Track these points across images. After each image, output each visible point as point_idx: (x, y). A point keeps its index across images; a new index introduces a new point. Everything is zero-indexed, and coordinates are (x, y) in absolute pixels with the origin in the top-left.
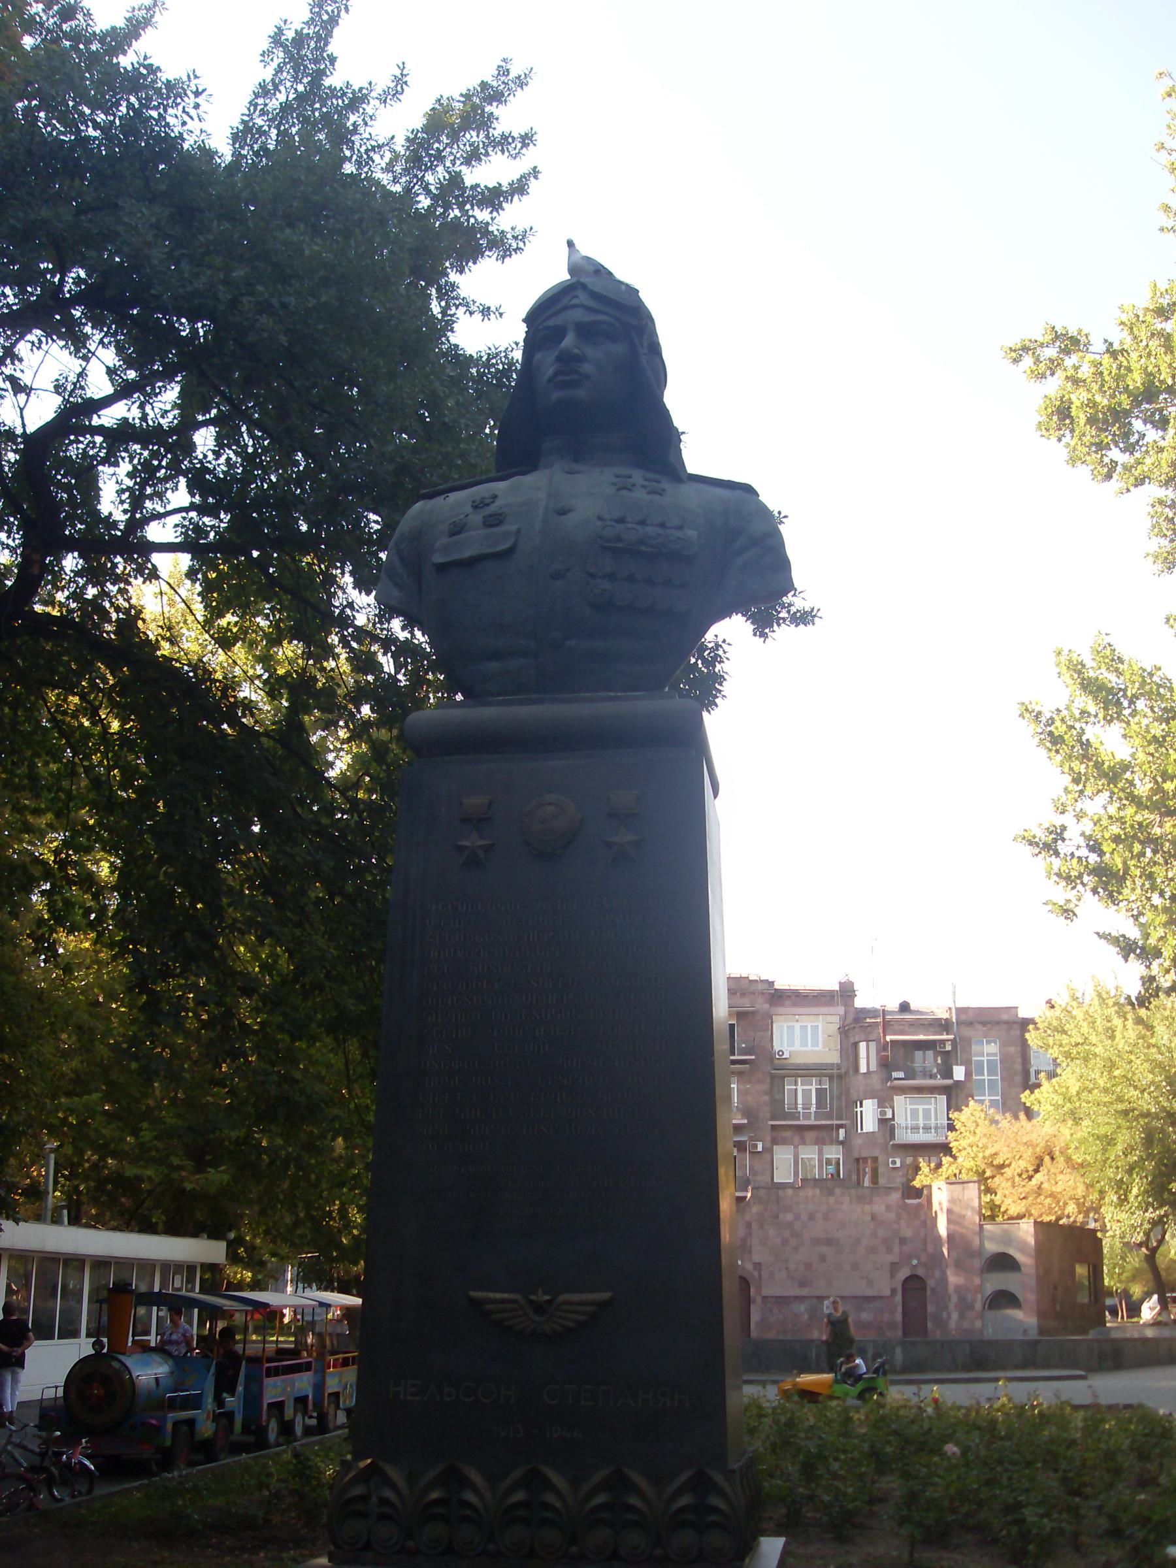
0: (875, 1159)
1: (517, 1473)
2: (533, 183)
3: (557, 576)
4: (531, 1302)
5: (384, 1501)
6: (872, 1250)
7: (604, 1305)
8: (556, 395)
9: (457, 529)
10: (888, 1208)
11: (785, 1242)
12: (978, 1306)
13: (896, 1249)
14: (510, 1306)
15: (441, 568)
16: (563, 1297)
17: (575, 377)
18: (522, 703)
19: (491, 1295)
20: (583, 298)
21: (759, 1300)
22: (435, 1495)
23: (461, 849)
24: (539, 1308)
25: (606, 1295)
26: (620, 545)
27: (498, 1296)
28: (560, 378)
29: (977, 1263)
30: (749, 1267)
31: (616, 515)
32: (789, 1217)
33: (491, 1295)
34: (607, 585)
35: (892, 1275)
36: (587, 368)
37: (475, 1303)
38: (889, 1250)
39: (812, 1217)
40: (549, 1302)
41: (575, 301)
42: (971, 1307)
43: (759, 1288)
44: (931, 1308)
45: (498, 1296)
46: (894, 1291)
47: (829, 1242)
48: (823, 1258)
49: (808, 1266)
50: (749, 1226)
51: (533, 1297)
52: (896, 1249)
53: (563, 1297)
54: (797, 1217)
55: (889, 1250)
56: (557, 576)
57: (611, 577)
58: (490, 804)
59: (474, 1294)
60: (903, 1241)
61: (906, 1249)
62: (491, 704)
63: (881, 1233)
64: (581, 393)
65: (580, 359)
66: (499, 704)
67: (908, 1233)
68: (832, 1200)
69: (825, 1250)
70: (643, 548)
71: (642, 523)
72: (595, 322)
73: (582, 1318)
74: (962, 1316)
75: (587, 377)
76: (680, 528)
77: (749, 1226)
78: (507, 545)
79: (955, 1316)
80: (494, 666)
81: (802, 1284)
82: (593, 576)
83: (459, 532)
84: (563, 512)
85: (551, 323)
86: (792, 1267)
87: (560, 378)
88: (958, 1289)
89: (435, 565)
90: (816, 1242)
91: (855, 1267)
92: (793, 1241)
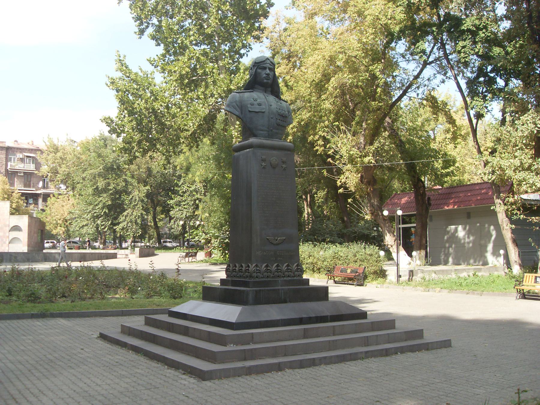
1: (276, 264)
3: (272, 118)
5: (257, 270)
7: (284, 239)
8: (265, 81)
9: (252, 105)
15: (250, 111)
18: (266, 139)
20: (268, 62)
22: (265, 269)
23: (262, 165)
57: (280, 120)
64: (270, 81)
66: (263, 139)
80: (262, 132)
84: (271, 106)
85: (264, 66)
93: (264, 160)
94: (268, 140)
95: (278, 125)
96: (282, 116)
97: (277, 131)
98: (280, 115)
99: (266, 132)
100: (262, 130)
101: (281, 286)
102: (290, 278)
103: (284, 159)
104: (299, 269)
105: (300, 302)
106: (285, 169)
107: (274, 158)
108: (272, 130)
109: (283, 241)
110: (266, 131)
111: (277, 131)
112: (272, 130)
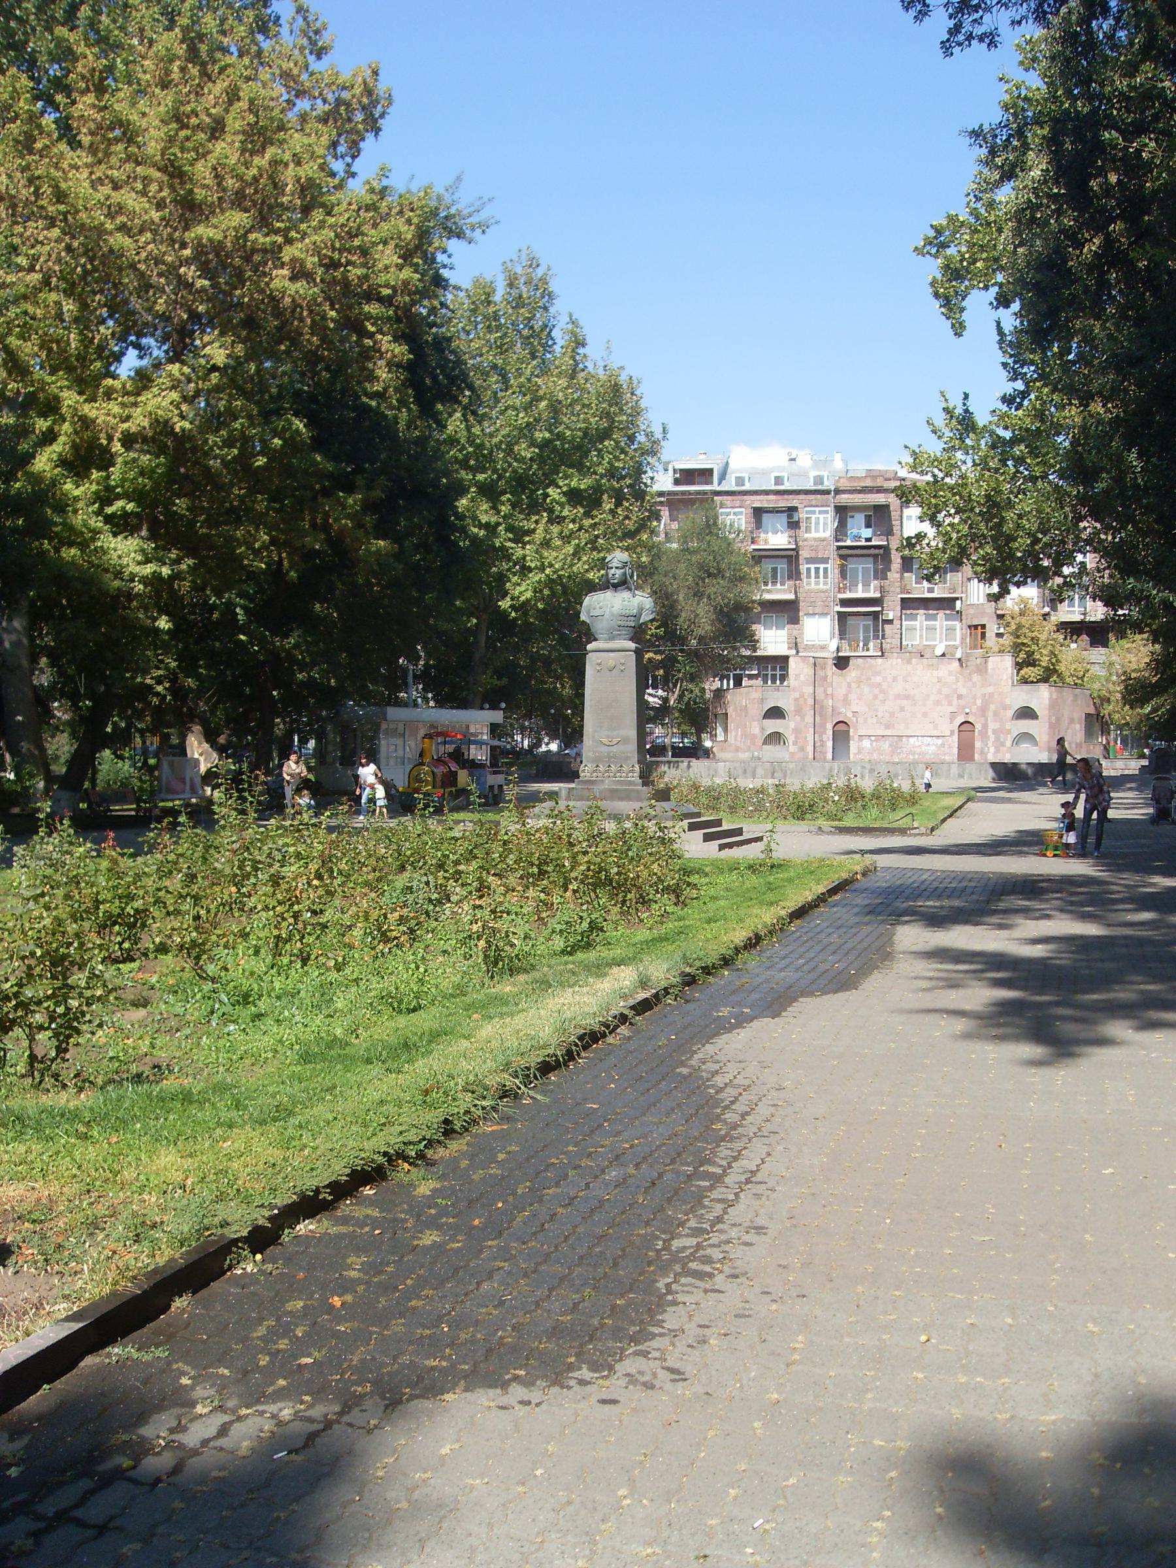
0: (983, 626)
6: (938, 703)
10: (950, 673)
11: (875, 697)
12: (1009, 743)
13: (955, 702)
21: (856, 737)
29: (1010, 713)
30: (850, 715)
32: (879, 679)
35: (952, 720)
38: (950, 704)
39: (895, 679)
42: (1003, 744)
43: (856, 730)
44: (978, 745)
46: (952, 733)
47: (907, 697)
48: (902, 709)
49: (892, 714)
50: (849, 686)
52: (955, 702)
54: (885, 679)
55: (950, 704)
60: (960, 697)
61: (962, 702)
63: (945, 691)
67: (963, 691)
68: (909, 667)
69: (904, 703)
74: (997, 751)
77: (849, 686)
79: (992, 750)
81: (888, 727)
86: (880, 714)
88: (994, 732)
90: (898, 697)
91: (925, 715)
92: (881, 697)
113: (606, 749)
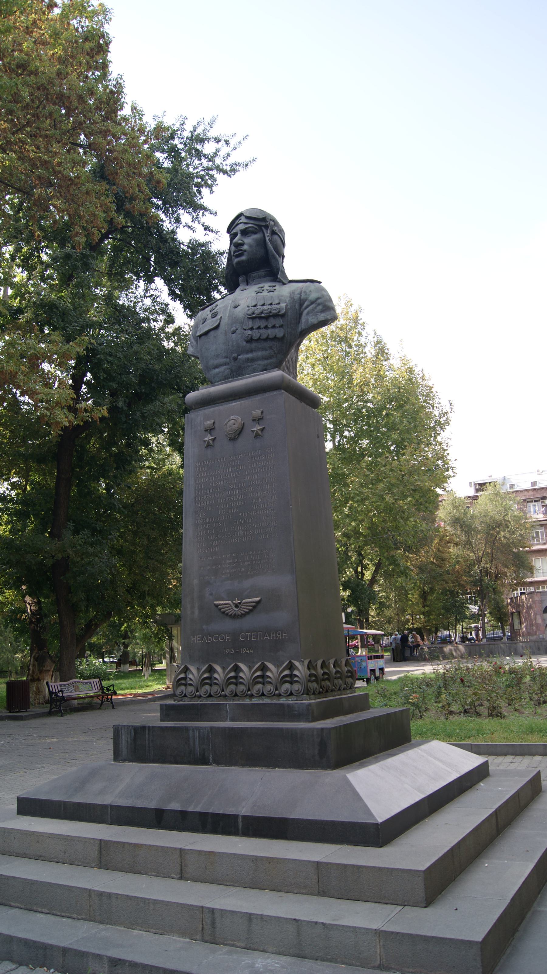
2: (241, 173)
3: (234, 332)
4: (234, 603)
5: (191, 679)
7: (258, 602)
14: (227, 605)
16: (244, 601)
17: (240, 252)
19: (221, 602)
24: (236, 606)
25: (258, 599)
26: (254, 316)
27: (223, 602)
28: (236, 254)
31: (254, 304)
33: (221, 602)
34: (250, 332)
36: (245, 247)
37: (217, 606)
40: (240, 603)
41: (241, 221)
45: (223, 602)
51: (234, 602)
53: (244, 601)
56: (234, 332)
57: (252, 329)
58: (214, 423)
59: (216, 602)
62: (216, 386)
65: (242, 245)
66: (219, 385)
70: (263, 315)
71: (264, 305)
72: (246, 228)
73: (251, 608)
75: (245, 251)
76: (279, 304)
78: (217, 324)
82: (245, 330)
83: (204, 322)
84: (236, 307)
87: (236, 254)
89: (198, 336)
93: (210, 430)
94: (231, 382)
95: (250, 340)
96: (260, 318)
97: (250, 356)
98: (253, 318)
99: (222, 369)
100: (217, 367)
101: (233, 720)
102: (267, 701)
103: (257, 413)
104: (296, 676)
105: (243, 765)
106: (257, 436)
107: (232, 417)
108: (235, 359)
109: (254, 607)
110: (225, 364)
111: (250, 356)
112: (235, 359)
113: (229, 625)
